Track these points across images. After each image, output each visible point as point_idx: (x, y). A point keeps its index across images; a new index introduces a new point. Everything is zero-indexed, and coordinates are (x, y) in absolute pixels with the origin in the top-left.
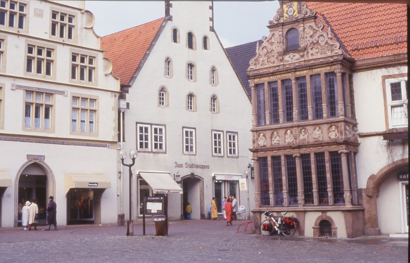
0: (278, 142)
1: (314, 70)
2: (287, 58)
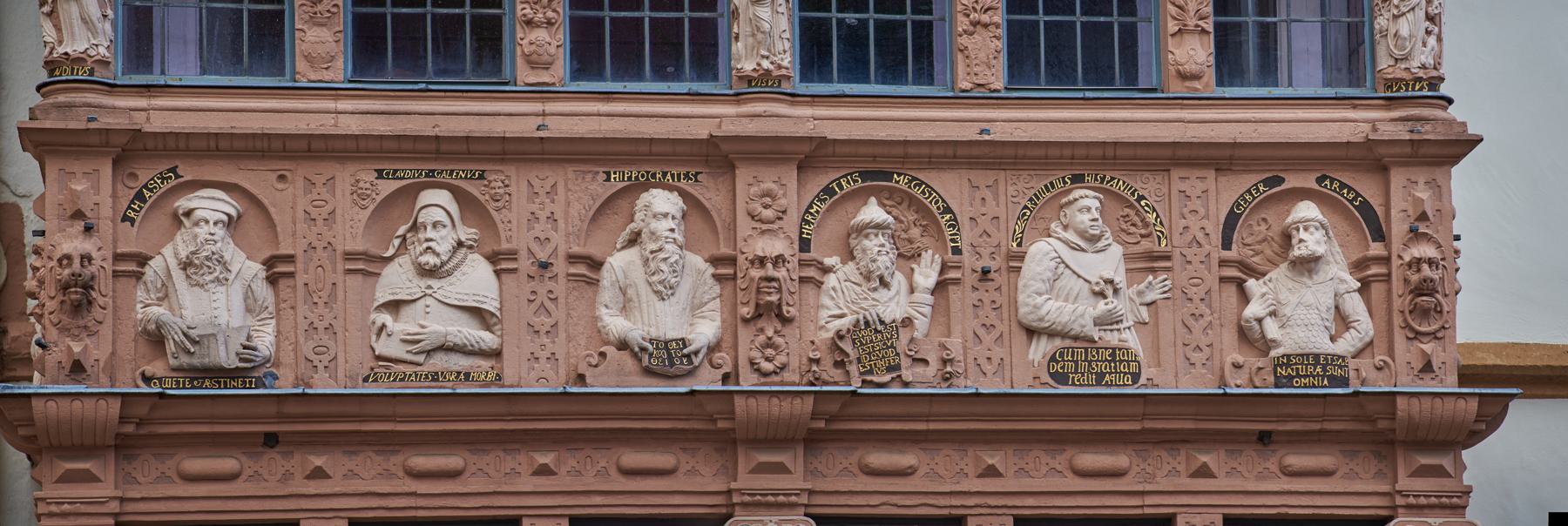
0: (488, 339)
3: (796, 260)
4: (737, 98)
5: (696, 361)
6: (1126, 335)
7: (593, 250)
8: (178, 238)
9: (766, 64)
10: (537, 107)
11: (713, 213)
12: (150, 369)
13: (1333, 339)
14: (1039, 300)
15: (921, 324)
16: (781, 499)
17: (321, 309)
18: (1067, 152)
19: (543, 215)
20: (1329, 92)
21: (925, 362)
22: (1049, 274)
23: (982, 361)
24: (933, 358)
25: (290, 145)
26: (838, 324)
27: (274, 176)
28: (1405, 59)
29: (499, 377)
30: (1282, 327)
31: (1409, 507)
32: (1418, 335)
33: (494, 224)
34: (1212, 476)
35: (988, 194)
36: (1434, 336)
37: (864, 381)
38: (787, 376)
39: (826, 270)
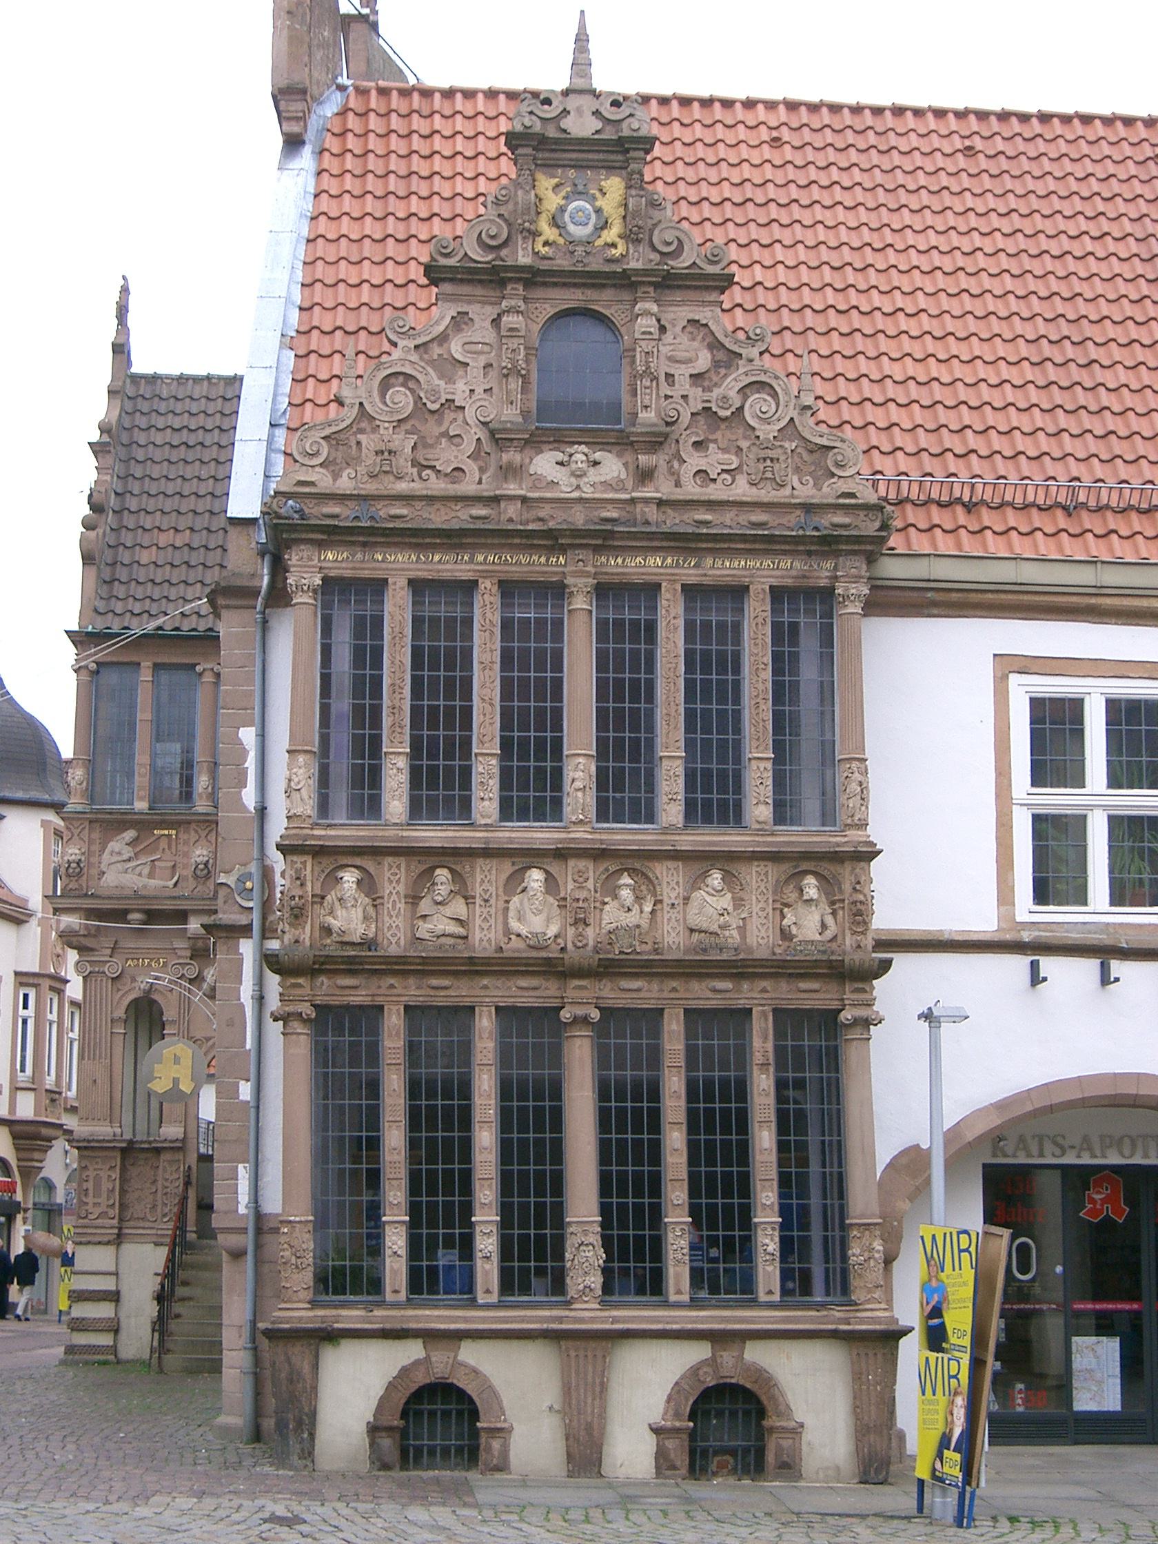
0: (460, 931)
1: (709, 562)
2: (545, 464)
36: (862, 933)
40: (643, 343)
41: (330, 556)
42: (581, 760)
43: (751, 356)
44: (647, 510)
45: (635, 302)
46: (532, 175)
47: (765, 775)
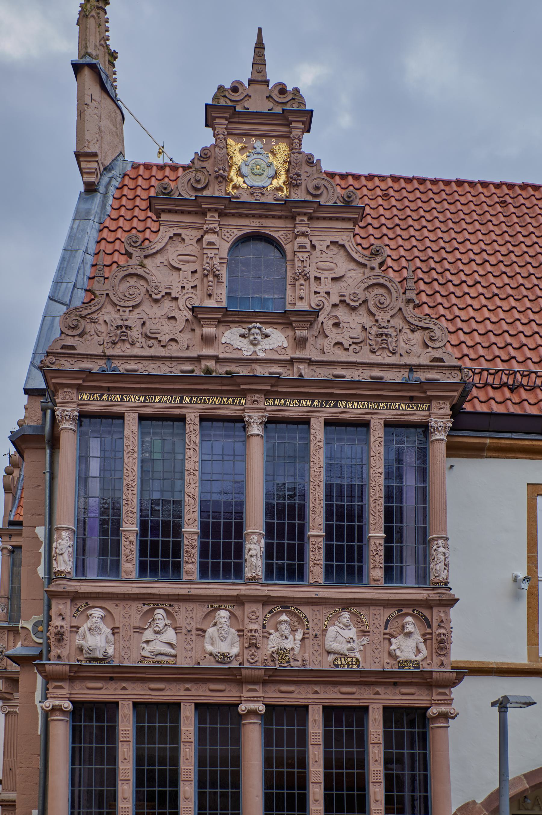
0: (173, 652)
1: (342, 404)
3: (261, 631)
4: (246, 584)
5: (231, 659)
6: (356, 654)
7: (204, 627)
8: (88, 622)
9: (254, 574)
10: (188, 586)
11: (238, 617)
12: (79, 658)
13: (415, 656)
14: (331, 643)
15: (297, 650)
16: (255, 699)
17: (126, 642)
18: (340, 601)
19: (189, 617)
20: (417, 586)
21: (298, 660)
22: (334, 636)
23: (314, 661)
24: (300, 660)
25: (119, 596)
26: (273, 649)
27: (115, 605)
28: (438, 576)
29: (176, 663)
30: (401, 652)
31: (436, 704)
32: (440, 655)
33: (176, 619)
34: (380, 694)
35: (317, 613)
36: (444, 655)
37: (280, 666)
38: (258, 664)
39: (270, 634)
40: (298, 254)
41: (85, 397)
42: (254, 536)
43: (374, 265)
44: (301, 367)
45: (295, 227)
46: (226, 140)
47: (379, 548)
